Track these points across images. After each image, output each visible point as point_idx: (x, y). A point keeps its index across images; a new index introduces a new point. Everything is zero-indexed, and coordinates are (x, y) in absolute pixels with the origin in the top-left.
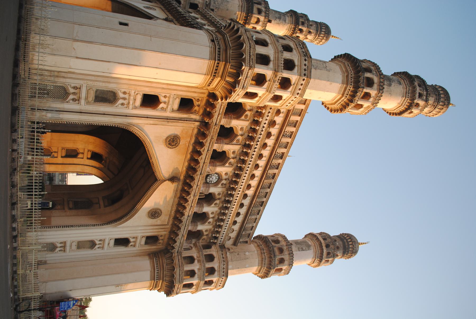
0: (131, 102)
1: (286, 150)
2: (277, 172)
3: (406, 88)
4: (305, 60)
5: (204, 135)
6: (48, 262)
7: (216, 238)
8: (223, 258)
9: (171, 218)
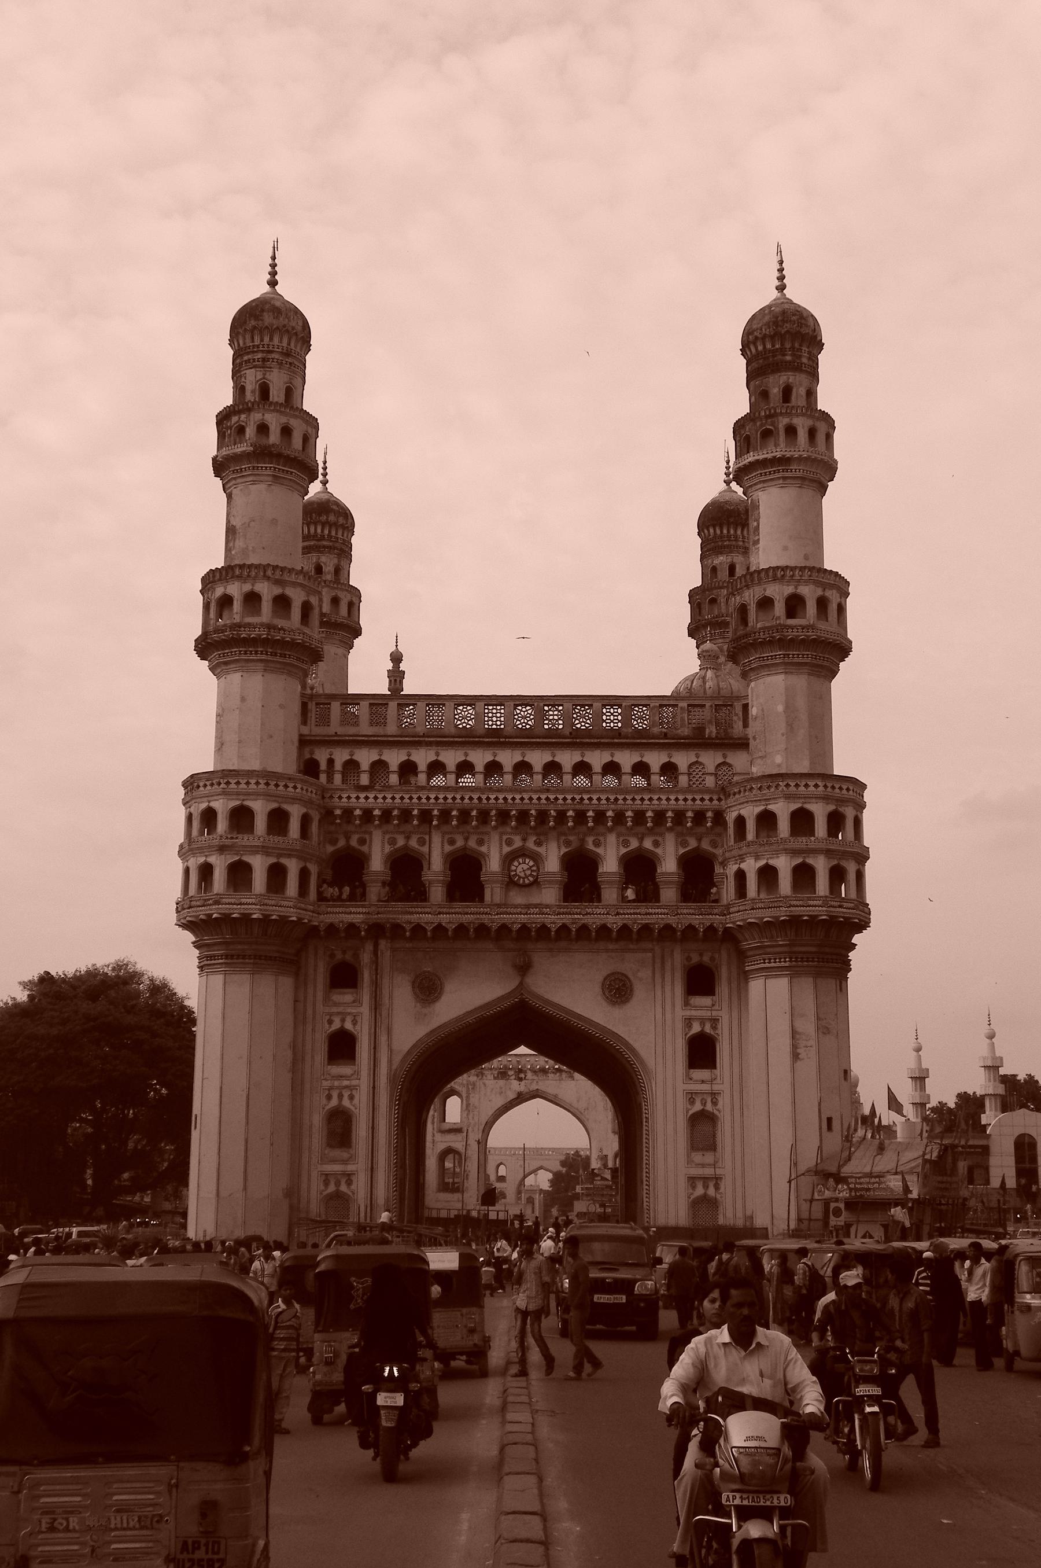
0: (346, 1083)
1: (447, 704)
2: (512, 704)
3: (235, 479)
4: (198, 787)
5: (397, 928)
6: (749, 1213)
7: (699, 816)
8: (740, 792)
9: (631, 946)
